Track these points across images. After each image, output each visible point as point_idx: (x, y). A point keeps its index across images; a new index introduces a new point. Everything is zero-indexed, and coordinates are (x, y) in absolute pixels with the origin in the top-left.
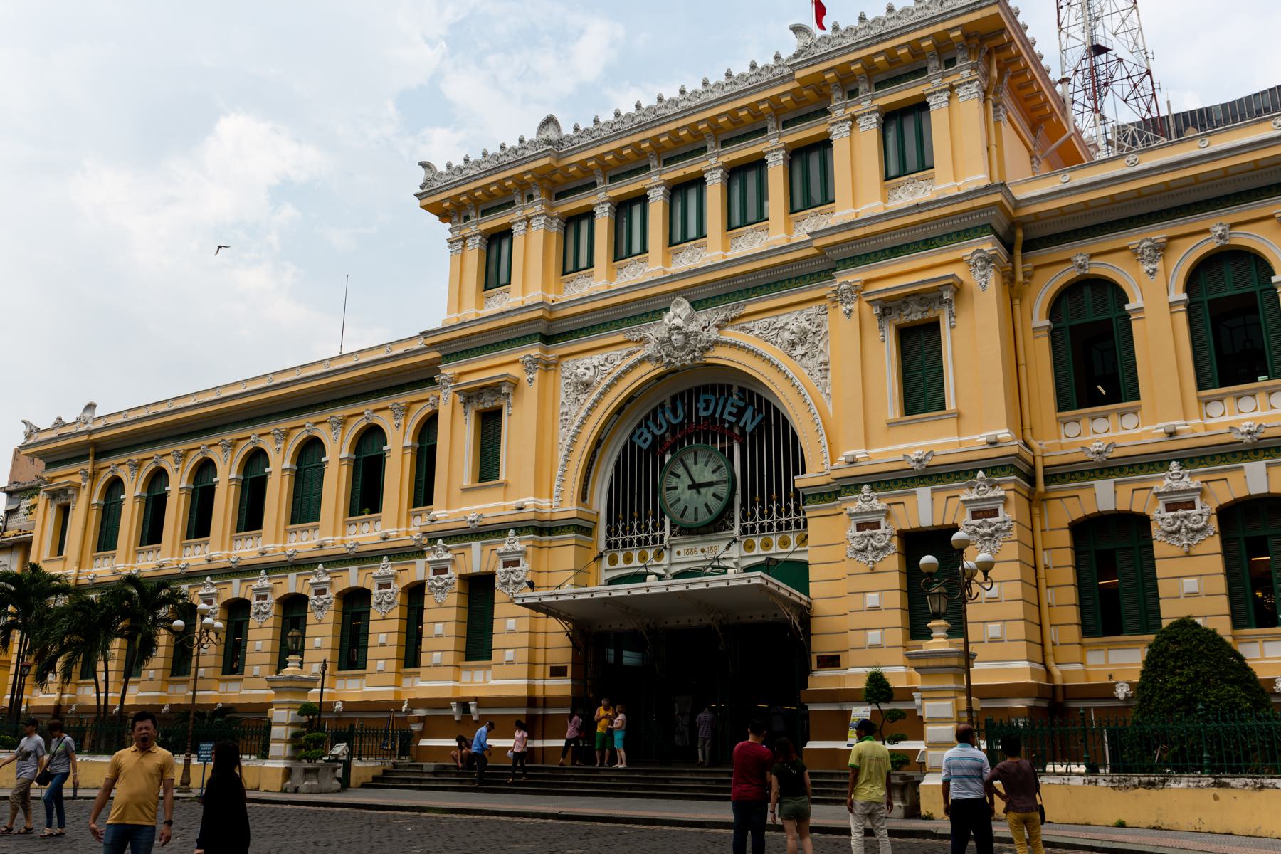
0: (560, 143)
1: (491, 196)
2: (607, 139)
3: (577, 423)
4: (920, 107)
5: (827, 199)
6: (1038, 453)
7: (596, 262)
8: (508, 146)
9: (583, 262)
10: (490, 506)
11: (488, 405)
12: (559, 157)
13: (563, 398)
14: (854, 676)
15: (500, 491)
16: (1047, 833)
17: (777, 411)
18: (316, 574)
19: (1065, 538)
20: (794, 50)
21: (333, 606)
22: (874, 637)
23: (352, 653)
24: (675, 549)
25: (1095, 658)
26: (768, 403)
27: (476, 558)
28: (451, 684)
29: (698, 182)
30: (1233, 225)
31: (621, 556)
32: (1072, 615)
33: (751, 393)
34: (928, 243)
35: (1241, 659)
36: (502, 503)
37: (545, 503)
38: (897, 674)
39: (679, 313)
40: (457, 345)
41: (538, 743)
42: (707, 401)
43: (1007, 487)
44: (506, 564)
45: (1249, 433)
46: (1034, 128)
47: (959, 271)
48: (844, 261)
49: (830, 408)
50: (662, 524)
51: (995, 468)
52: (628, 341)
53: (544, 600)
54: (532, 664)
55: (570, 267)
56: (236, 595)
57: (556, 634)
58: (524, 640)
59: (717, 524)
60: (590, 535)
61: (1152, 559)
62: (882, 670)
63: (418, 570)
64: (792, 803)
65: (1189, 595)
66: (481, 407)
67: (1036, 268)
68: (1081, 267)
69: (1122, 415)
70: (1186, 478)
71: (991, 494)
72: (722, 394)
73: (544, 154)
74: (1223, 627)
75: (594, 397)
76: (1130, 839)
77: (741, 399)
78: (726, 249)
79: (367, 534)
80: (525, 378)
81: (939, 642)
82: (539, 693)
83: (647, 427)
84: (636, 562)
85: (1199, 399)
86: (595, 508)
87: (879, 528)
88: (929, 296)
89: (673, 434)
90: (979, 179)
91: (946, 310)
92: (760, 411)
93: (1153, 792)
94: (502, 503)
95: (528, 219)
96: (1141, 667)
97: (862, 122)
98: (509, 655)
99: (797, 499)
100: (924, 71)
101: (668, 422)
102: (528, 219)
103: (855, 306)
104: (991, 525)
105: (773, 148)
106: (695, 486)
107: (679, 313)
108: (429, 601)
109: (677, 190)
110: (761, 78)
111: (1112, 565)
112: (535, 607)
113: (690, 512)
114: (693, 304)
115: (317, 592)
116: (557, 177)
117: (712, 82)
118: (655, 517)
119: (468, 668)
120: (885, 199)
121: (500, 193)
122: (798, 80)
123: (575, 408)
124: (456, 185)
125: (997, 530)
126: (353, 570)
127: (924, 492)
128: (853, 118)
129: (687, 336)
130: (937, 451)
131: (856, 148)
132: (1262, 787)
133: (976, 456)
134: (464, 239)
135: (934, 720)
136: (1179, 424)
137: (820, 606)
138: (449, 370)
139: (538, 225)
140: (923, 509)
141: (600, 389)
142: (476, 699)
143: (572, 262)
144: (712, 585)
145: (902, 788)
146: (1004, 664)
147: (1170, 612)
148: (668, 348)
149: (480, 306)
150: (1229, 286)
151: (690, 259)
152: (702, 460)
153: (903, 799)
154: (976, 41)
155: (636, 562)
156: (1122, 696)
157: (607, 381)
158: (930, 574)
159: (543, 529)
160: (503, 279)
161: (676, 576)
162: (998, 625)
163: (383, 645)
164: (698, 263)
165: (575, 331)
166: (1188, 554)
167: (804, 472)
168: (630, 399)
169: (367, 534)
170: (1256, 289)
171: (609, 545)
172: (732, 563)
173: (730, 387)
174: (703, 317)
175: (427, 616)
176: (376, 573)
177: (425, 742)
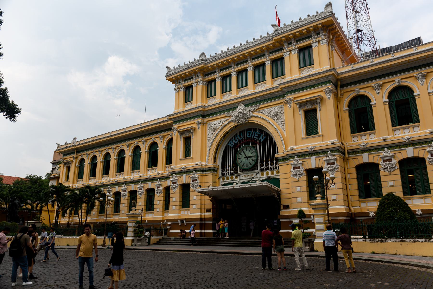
0: (206, 60)
1: (186, 76)
2: (219, 59)
3: (212, 140)
4: (309, 47)
5: (283, 74)
6: (346, 146)
7: (217, 94)
8: (191, 62)
9: (213, 94)
10: (188, 164)
11: (187, 135)
12: (206, 64)
13: (208, 133)
14: (294, 211)
15: (191, 160)
16: (354, 255)
17: (270, 135)
18: (139, 184)
19: (354, 170)
20: (273, 32)
21: (144, 193)
22: (299, 200)
23: (150, 206)
24: (241, 176)
25: (363, 205)
26: (267, 133)
27: (184, 179)
28: (178, 215)
29: (246, 70)
30: (402, 79)
31: (225, 178)
32: (357, 192)
33: (262, 130)
34: (313, 86)
35: (407, 204)
37: (204, 163)
38: (306, 210)
40: (178, 119)
41: (203, 231)
42: (249, 133)
43: (337, 156)
44: (193, 181)
45: (408, 139)
46: (342, 53)
47: (322, 94)
48: (288, 92)
49: (285, 134)
50: (237, 168)
51: (333, 151)
52: (226, 116)
53: (204, 190)
54: (201, 209)
55: (209, 95)
56: (133, 189)
57: (208, 200)
58: (199, 202)
59: (253, 168)
60: (217, 172)
61: (380, 176)
62: (302, 209)
63: (168, 183)
64: (280, 247)
65: (391, 186)
66: (185, 136)
67: (344, 93)
68: (357, 92)
69: (370, 135)
70: (389, 153)
71: (333, 158)
72: (254, 131)
73: (201, 64)
74: (401, 195)
75: (217, 132)
76: (377, 257)
77: (260, 132)
78: (254, 89)
79: (153, 173)
80: (197, 127)
81: (318, 201)
82: (203, 217)
83: (232, 141)
84: (230, 179)
85: (393, 130)
86: (218, 164)
87: (300, 168)
88: (313, 101)
89: (240, 143)
90: (327, 67)
91: (318, 105)
92: (265, 135)
93: (383, 243)
95: (197, 82)
96: (377, 207)
97: (293, 52)
98: (194, 206)
99: (276, 160)
100: (310, 37)
101: (238, 139)
102: (197, 82)
103: (292, 105)
104: (332, 167)
105: (267, 60)
106: (247, 157)
107: (241, 108)
108: (171, 192)
109: (240, 73)
110: (263, 40)
111: (368, 178)
112: (202, 193)
113: (245, 165)
114: (245, 105)
115: (140, 190)
116: (205, 70)
117: (249, 42)
118: (235, 166)
119: (183, 210)
120: (300, 74)
121: (189, 75)
122: (274, 40)
123: (212, 136)
124: (177, 73)
125: (334, 168)
126: (150, 183)
127: (313, 158)
128: (290, 51)
129: (243, 114)
130: (316, 146)
131: (291, 59)
132: (415, 241)
133: (328, 147)
134: (179, 88)
135: (318, 223)
136: (387, 137)
137: (283, 191)
138: (175, 126)
139: (200, 84)
140: (313, 163)
141: (219, 130)
142: (185, 219)
143: (210, 94)
144: (252, 186)
145: (309, 243)
146: (337, 207)
147: (385, 191)
149: (184, 107)
150: (401, 97)
151: (244, 92)
152: (248, 150)
153: (309, 246)
154: (326, 27)
155: (230, 179)
156: (371, 216)
157: (221, 128)
158: (316, 181)
159: (203, 170)
160: (190, 100)
161: (242, 183)
162: (335, 196)
163: (159, 204)
164: (246, 93)
165: (211, 114)
166: (390, 175)
167: (278, 153)
168: (227, 133)
169: (153, 173)
170: (409, 97)
171: (222, 175)
172: (258, 179)
173: (256, 129)
174: (248, 109)
175: (171, 196)
176: (156, 184)
177: (171, 231)
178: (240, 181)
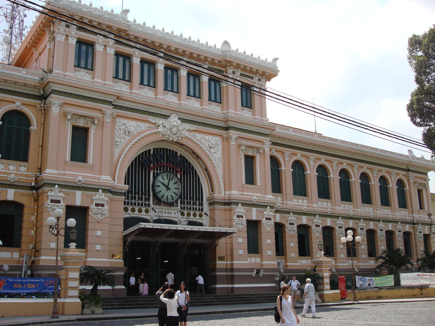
11: (81, 125)
36: (91, 175)
39: (174, 120)
42: (173, 156)
44: (97, 205)
48: (232, 127)
94: (91, 175)
127: (254, 209)
148: (169, 132)
173: (176, 153)
178: (152, 216)
